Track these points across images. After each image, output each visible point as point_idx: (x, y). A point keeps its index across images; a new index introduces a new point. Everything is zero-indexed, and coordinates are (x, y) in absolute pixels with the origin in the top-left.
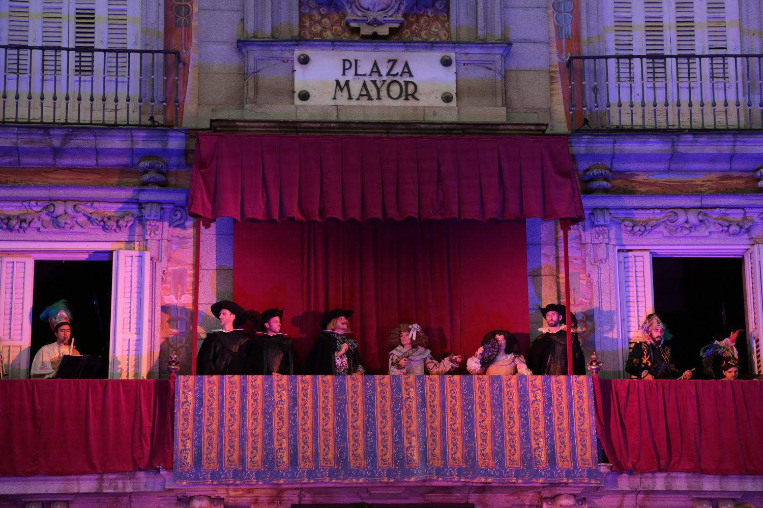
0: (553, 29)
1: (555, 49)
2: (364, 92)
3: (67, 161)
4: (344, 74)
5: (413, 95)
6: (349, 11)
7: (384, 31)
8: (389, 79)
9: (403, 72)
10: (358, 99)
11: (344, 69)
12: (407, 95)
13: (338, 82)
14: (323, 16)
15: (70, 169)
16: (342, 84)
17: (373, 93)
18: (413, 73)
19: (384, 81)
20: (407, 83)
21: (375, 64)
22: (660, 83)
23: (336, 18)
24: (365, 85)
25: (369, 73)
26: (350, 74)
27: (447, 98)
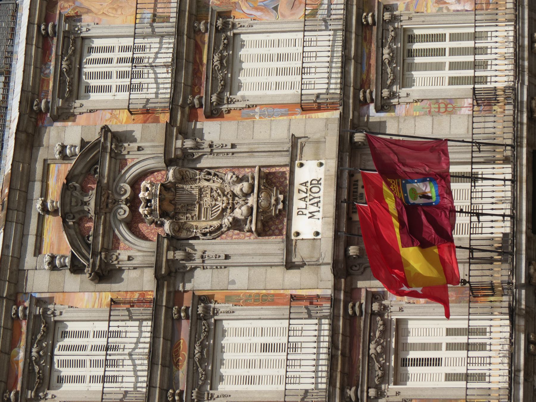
0: (281, 118)
1: (293, 117)
2: (316, 205)
3: (347, 351)
4: (306, 214)
5: (318, 181)
6: (270, 214)
7: (281, 197)
8: (309, 193)
9: (305, 186)
10: (319, 208)
11: (303, 214)
12: (318, 184)
13: (309, 217)
14: (270, 229)
15: (350, 350)
16: (311, 215)
17: (316, 200)
18: (306, 181)
19: (310, 195)
20: (311, 184)
21: (300, 199)
22: (313, 70)
23: (271, 223)
24: (312, 204)
25: (305, 203)
26: (305, 211)
27: (321, 164)
